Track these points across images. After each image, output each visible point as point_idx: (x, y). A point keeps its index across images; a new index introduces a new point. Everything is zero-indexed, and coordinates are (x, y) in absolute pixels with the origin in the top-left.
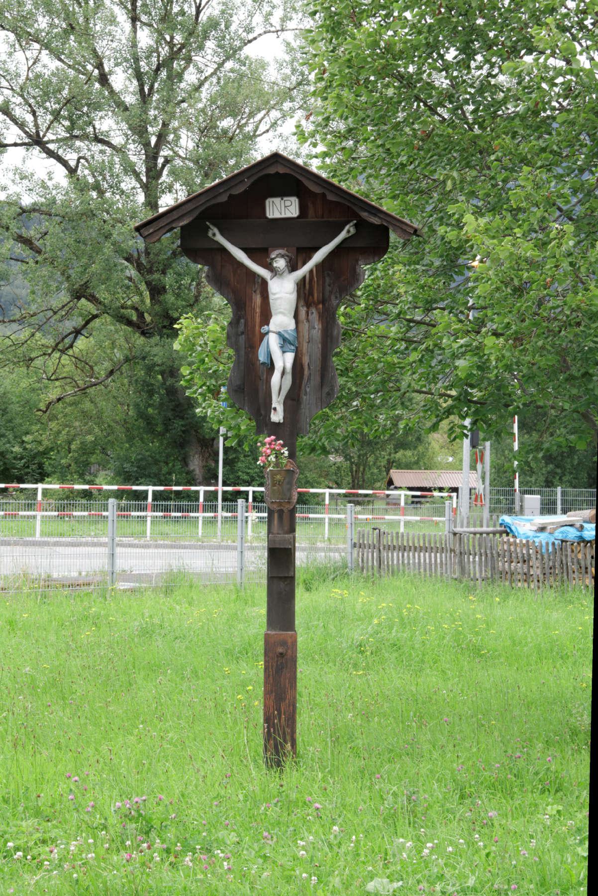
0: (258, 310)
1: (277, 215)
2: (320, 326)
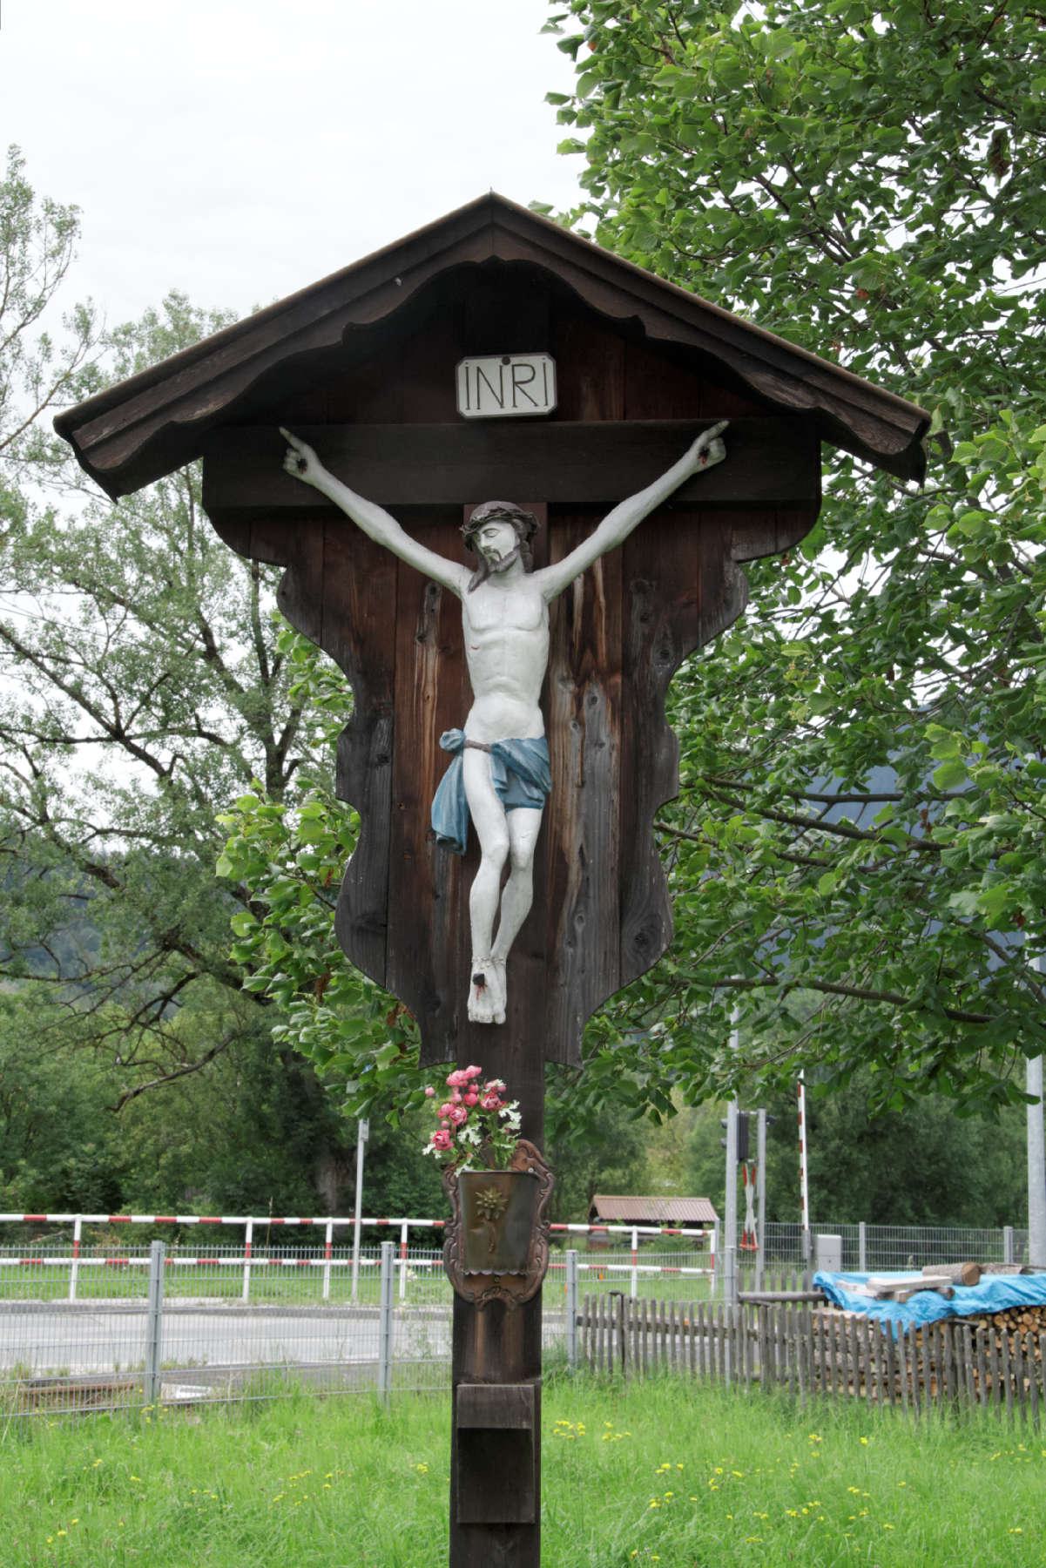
0: (430, 691)
1: (490, 409)
2: (617, 740)
